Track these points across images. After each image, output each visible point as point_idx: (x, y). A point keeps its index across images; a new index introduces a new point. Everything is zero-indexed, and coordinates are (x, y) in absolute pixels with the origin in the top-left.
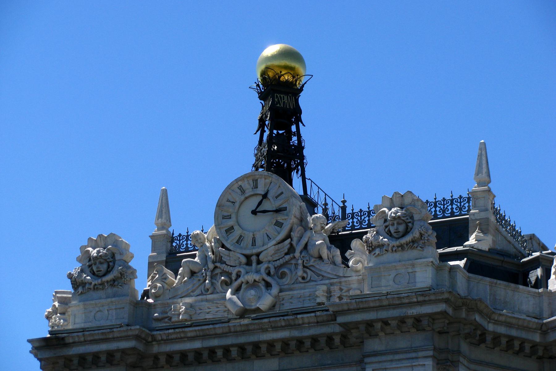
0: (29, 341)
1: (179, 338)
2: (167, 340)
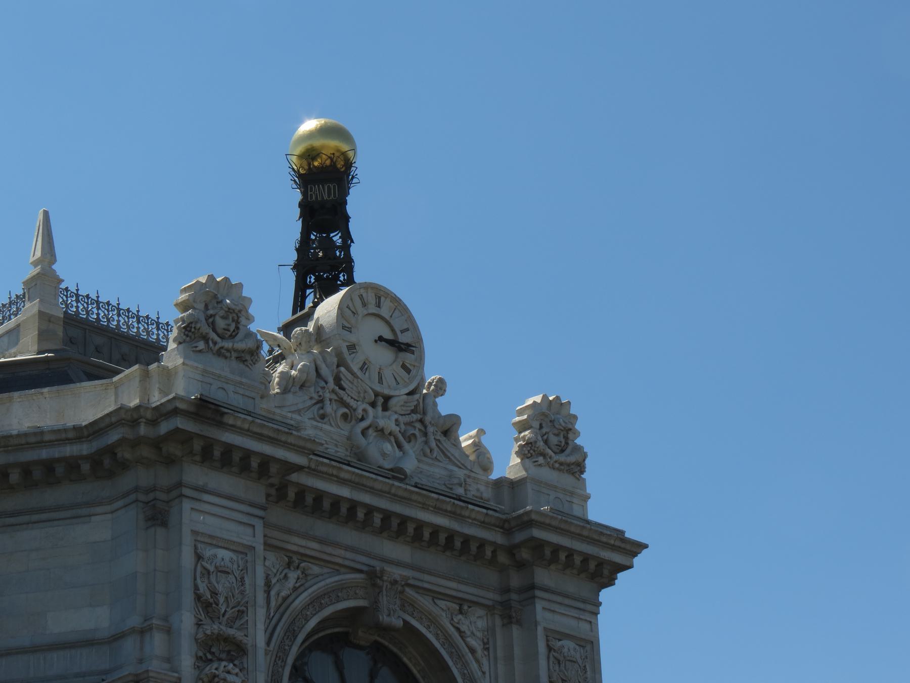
1: (328, 474)
2: (314, 470)
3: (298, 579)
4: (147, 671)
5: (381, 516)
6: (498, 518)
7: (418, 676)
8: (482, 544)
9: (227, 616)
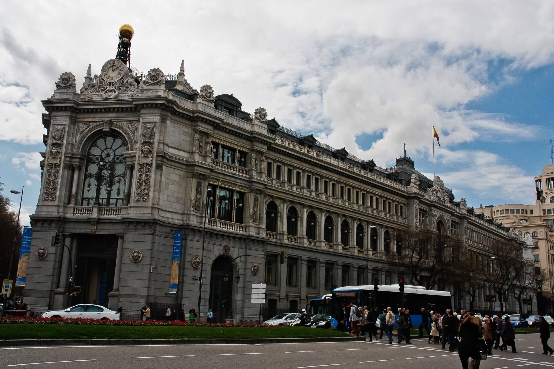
0: (42, 101)
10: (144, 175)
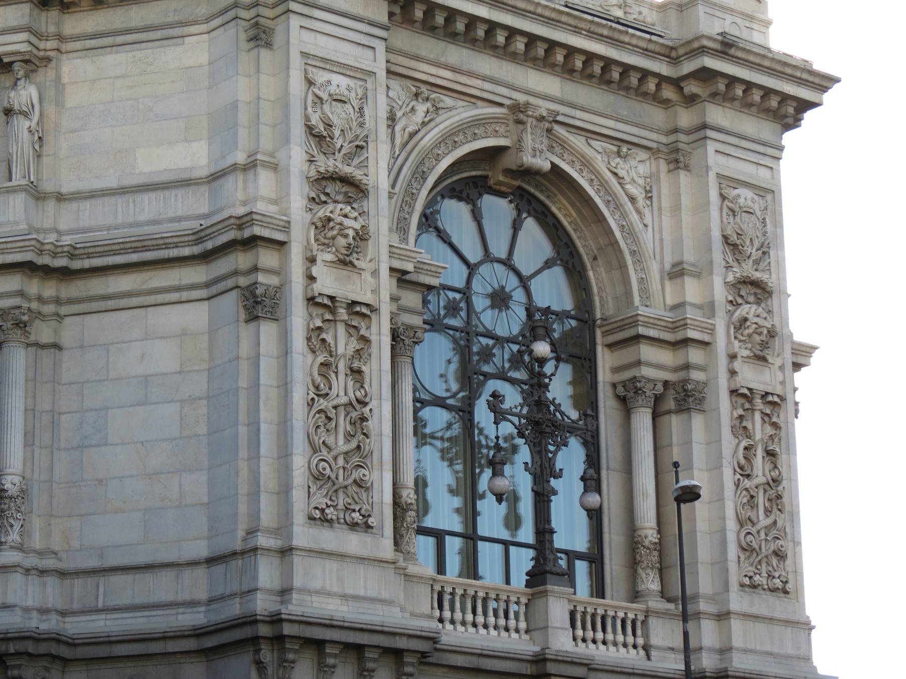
3: (428, 112)
4: (251, 213)
5: (525, 40)
6: (662, 45)
7: (569, 228)
8: (645, 74)
9: (343, 152)
10: (760, 453)
